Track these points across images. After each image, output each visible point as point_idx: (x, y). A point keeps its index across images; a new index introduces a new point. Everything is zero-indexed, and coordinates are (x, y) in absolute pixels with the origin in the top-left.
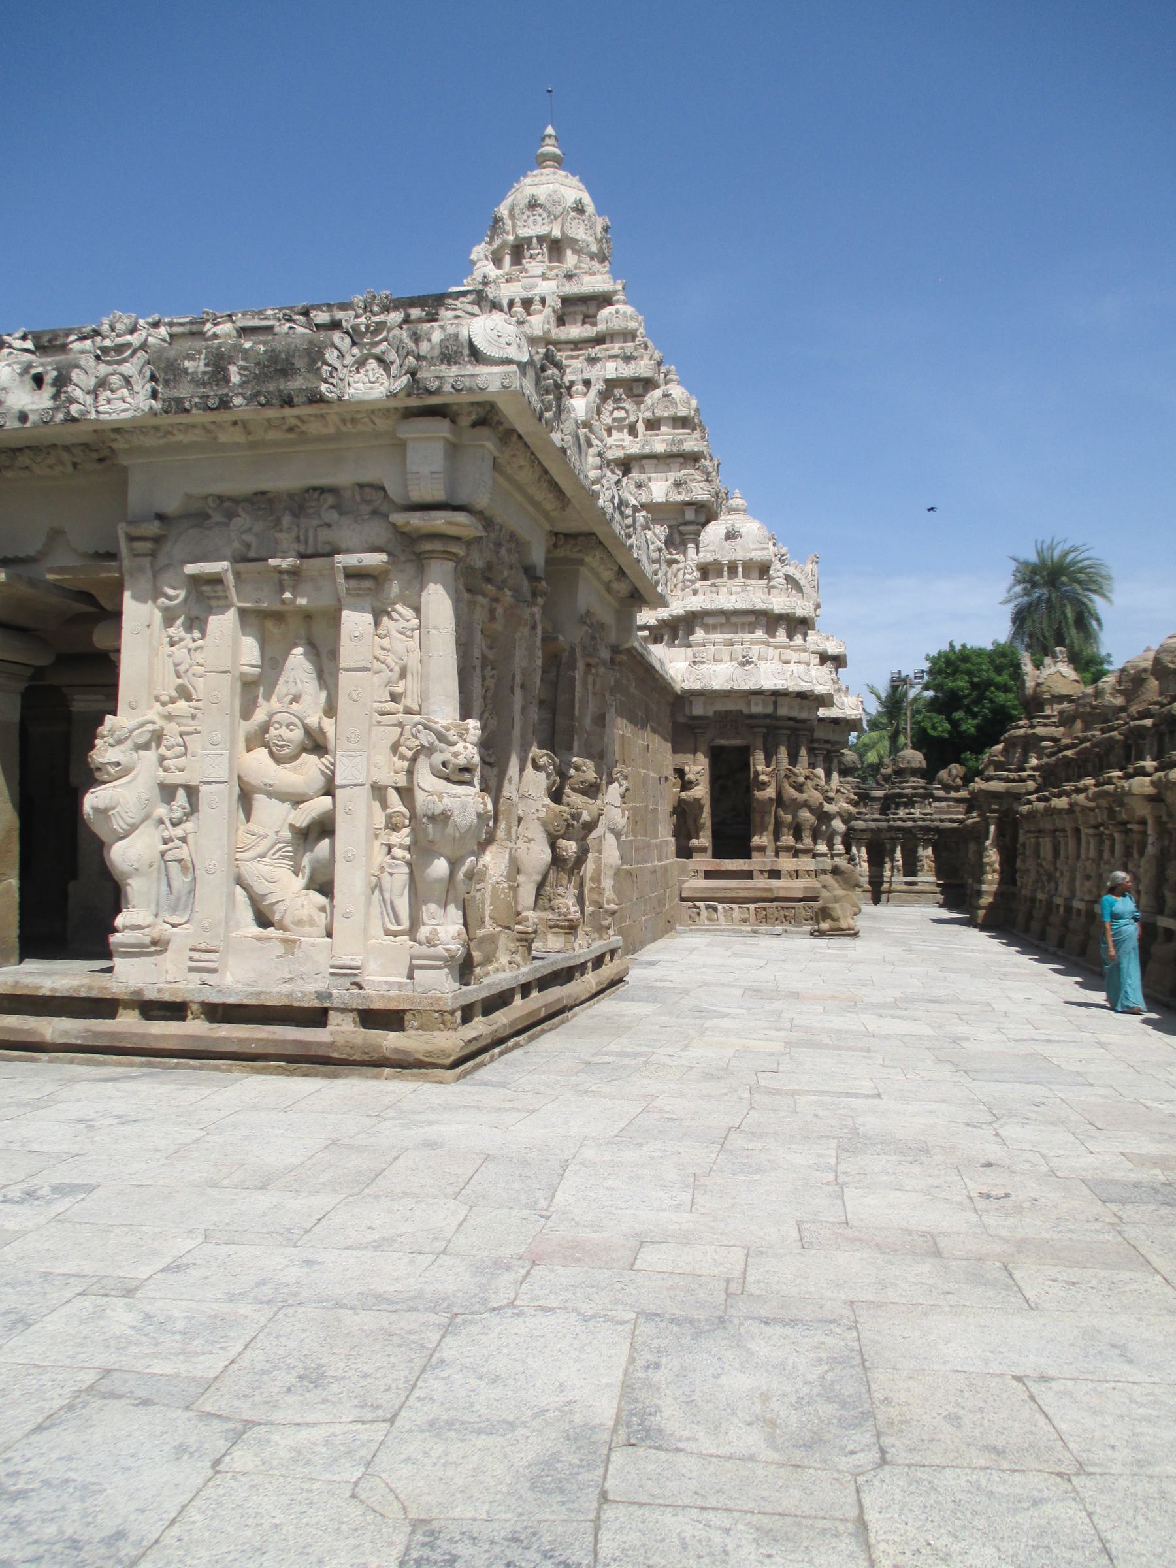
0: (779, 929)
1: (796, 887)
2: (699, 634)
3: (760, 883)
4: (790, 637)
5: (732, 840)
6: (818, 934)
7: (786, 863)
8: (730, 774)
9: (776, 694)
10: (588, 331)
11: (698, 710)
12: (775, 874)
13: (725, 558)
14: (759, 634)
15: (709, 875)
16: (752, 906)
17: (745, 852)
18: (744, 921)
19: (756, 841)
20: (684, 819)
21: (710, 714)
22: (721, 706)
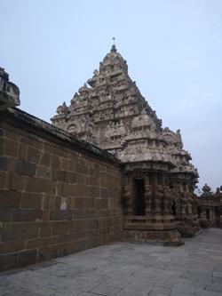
0: (154, 241)
1: (161, 226)
2: (129, 146)
3: (148, 224)
4: (157, 145)
5: (140, 210)
6: (166, 244)
7: (158, 217)
8: (139, 185)
9: (151, 162)
10: (115, 82)
11: (128, 168)
12: (154, 221)
13: (138, 126)
14: (146, 144)
15: (133, 221)
16: (146, 232)
17: (143, 213)
18: (143, 237)
19: (147, 210)
20: (124, 202)
21: (132, 169)
22: (135, 167)
